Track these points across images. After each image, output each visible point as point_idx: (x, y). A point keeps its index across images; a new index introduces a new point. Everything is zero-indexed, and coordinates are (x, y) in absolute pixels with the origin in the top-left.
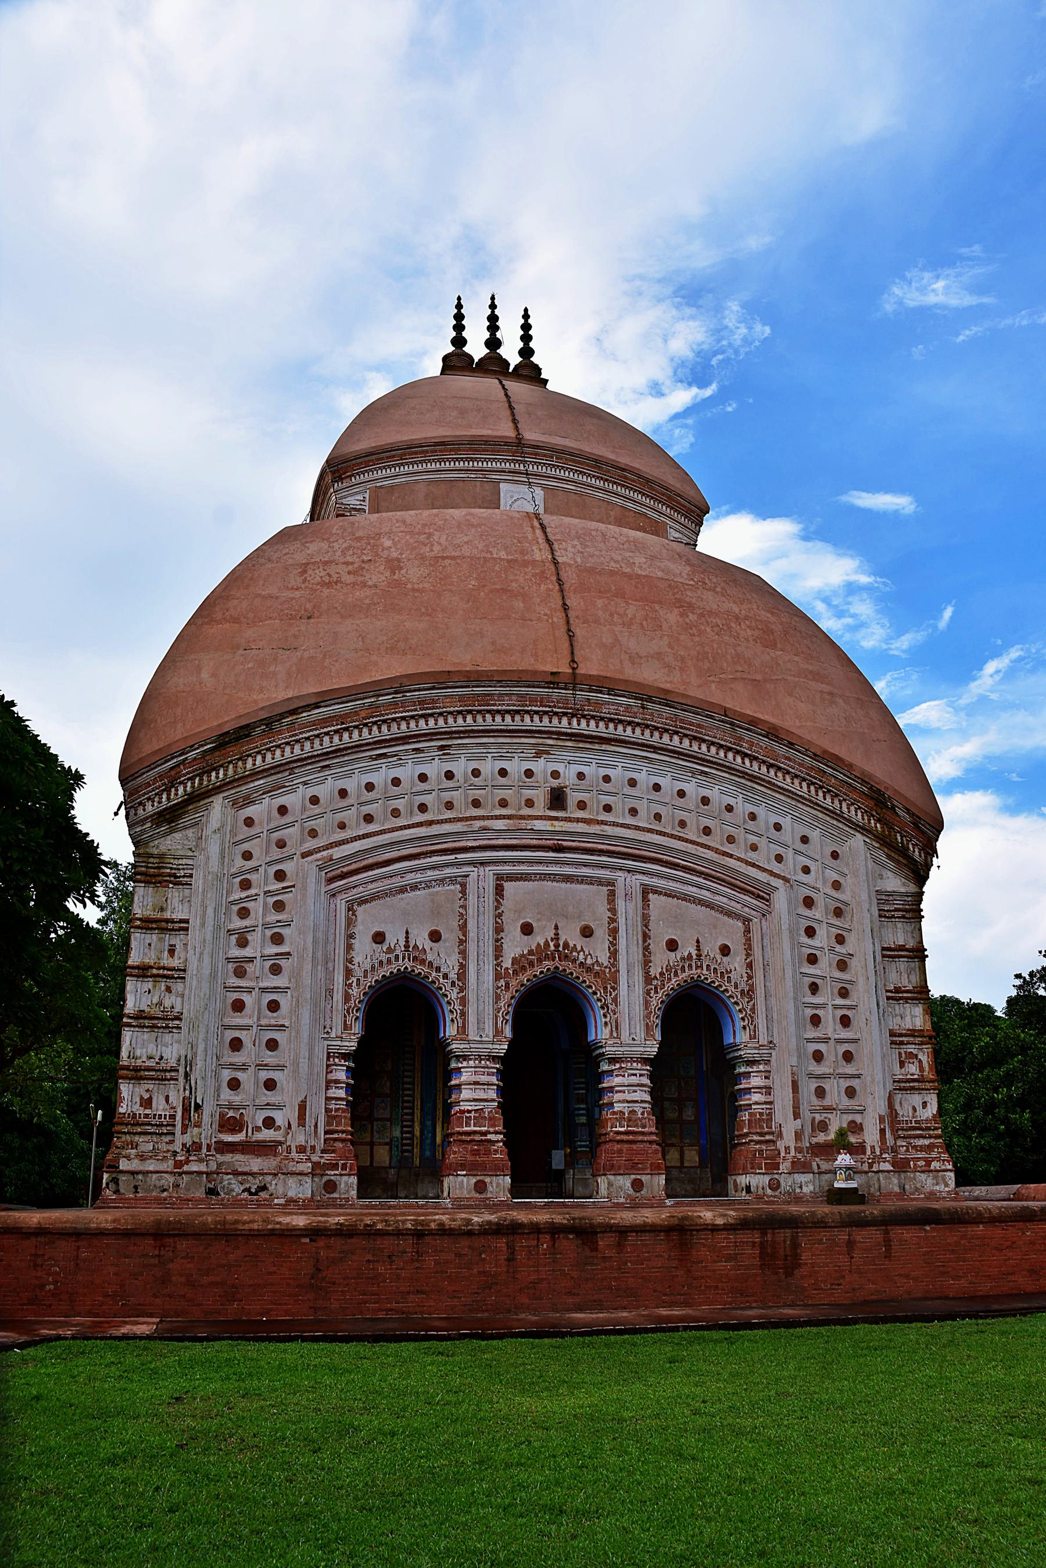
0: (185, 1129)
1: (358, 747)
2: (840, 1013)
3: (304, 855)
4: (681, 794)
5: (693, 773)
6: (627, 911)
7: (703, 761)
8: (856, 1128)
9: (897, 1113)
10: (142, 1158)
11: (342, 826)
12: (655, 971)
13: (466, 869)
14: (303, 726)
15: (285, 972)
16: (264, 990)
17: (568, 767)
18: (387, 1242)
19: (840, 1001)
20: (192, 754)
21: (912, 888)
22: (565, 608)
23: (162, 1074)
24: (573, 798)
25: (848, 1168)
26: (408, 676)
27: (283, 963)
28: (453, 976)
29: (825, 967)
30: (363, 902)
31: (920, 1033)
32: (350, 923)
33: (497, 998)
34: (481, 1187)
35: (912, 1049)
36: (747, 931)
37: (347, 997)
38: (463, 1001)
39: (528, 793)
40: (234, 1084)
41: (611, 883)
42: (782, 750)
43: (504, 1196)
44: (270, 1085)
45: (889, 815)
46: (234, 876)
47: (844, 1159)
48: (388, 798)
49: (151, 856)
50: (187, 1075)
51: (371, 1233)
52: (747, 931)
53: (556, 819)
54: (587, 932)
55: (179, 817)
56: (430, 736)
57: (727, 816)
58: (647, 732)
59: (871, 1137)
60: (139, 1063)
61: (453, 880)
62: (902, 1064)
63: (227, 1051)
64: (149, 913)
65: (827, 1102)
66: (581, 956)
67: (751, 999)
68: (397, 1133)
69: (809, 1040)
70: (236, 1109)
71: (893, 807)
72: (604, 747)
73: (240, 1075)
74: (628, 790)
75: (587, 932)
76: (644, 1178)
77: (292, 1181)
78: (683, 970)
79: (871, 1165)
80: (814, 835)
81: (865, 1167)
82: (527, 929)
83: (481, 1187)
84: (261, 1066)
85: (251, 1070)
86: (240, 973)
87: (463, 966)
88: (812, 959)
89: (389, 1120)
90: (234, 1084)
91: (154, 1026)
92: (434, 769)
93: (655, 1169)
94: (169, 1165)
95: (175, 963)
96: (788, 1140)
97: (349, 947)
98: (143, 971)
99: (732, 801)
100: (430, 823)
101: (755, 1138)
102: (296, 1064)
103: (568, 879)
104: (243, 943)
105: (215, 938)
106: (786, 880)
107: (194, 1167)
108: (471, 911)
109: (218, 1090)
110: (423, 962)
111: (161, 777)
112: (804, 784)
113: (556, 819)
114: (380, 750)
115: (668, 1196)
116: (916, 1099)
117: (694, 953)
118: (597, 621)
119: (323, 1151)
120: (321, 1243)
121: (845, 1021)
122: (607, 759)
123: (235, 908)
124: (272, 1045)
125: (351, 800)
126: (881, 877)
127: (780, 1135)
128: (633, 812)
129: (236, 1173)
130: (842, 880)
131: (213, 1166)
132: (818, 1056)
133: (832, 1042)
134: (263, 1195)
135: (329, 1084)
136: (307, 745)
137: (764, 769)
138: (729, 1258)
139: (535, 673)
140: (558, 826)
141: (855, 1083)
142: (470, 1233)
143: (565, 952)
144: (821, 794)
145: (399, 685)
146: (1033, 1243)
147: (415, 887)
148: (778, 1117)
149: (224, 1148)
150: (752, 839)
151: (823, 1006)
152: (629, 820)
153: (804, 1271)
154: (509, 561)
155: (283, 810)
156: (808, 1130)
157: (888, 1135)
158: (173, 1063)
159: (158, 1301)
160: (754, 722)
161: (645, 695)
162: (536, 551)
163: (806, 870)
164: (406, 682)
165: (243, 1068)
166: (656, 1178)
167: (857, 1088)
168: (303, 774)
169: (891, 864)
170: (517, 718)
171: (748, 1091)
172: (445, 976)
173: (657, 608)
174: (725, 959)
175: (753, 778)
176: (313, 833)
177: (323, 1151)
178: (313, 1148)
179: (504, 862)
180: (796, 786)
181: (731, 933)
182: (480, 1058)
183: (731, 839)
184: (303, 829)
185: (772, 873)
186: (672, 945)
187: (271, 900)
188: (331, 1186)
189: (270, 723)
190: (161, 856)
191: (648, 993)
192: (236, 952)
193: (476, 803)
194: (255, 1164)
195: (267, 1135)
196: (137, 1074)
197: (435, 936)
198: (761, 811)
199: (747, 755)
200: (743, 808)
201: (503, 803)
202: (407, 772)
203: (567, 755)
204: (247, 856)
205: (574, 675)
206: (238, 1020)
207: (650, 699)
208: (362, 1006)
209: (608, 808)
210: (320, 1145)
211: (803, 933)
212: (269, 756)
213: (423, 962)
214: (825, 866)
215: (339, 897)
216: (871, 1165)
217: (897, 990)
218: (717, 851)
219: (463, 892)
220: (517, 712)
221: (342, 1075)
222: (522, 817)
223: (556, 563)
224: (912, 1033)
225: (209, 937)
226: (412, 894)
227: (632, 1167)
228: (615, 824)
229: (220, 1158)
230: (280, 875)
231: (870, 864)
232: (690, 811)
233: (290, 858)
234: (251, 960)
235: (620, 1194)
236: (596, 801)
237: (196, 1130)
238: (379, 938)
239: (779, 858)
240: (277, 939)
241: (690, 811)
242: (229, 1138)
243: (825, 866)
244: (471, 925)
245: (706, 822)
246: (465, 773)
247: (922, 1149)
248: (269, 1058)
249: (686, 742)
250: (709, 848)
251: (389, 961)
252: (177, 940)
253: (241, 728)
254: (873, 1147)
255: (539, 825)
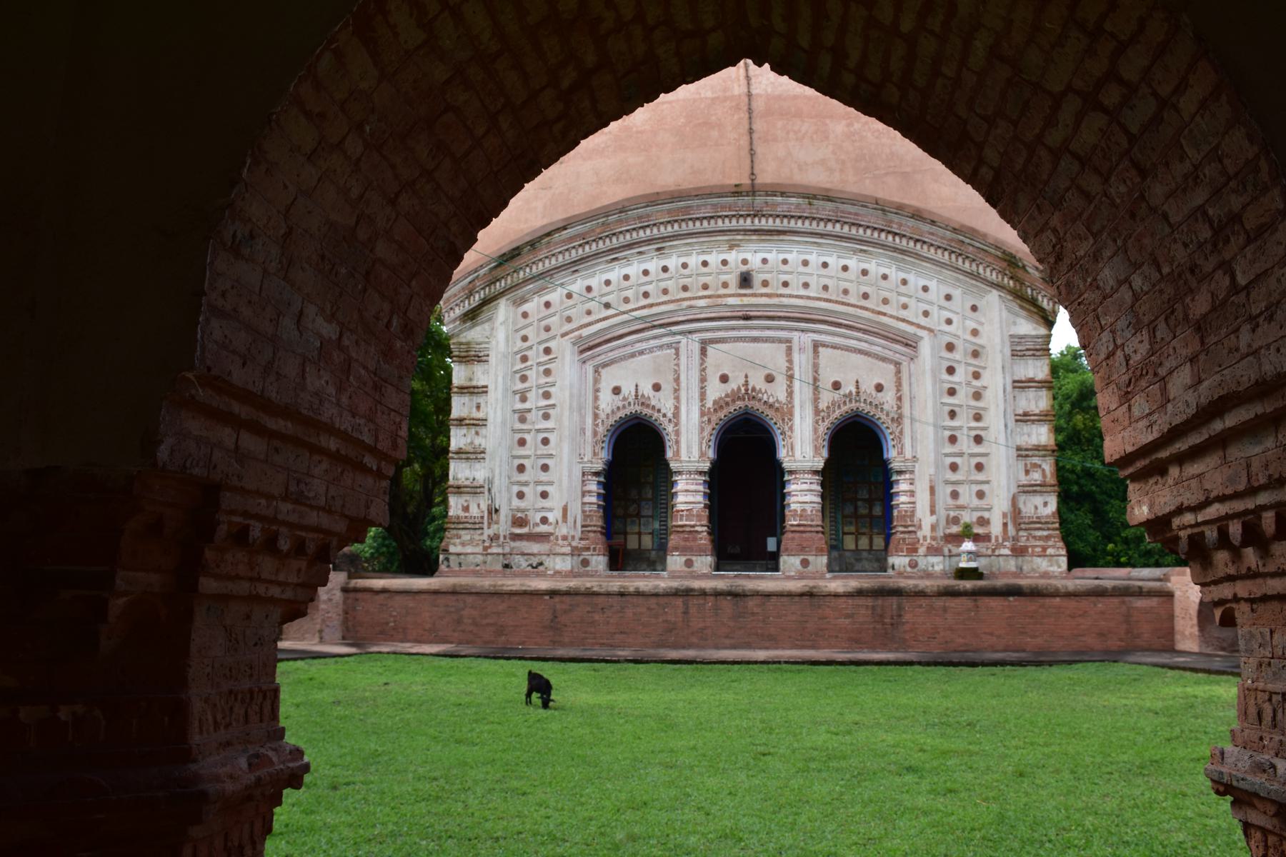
0: (489, 524)
1: (597, 255)
2: (974, 433)
3: (563, 335)
4: (845, 268)
5: (855, 251)
6: (802, 362)
7: (861, 242)
8: (983, 522)
9: (1020, 512)
10: (463, 544)
11: (589, 313)
12: (823, 405)
13: (678, 337)
14: (557, 243)
15: (552, 418)
16: (538, 431)
17: (753, 255)
18: (601, 599)
19: (974, 424)
20: (482, 272)
21: (1042, 331)
22: (751, 131)
23: (475, 490)
24: (757, 279)
25: (970, 553)
26: (628, 200)
27: (551, 411)
28: (670, 415)
29: (962, 398)
30: (605, 365)
31: (1045, 448)
32: (596, 381)
33: (702, 430)
34: (689, 563)
35: (1036, 460)
36: (898, 372)
37: (595, 433)
38: (677, 433)
39: (724, 278)
40: (521, 495)
41: (789, 341)
42: (926, 227)
43: (706, 570)
44: (544, 495)
45: (1020, 274)
46: (516, 353)
47: (968, 546)
48: (621, 290)
49: (461, 344)
50: (489, 490)
51: (590, 594)
52: (898, 372)
53: (745, 295)
54: (770, 379)
55: (477, 315)
56: (649, 241)
57: (883, 283)
58: (814, 223)
59: (996, 529)
60: (460, 483)
61: (669, 346)
62: (1027, 472)
63: (515, 473)
64: (464, 383)
65: (961, 502)
66: (765, 398)
67: (899, 424)
68: (657, 525)
69: (946, 455)
70: (523, 511)
71: (1024, 267)
72: (781, 237)
73: (524, 489)
74: (802, 269)
75: (770, 379)
76: (811, 558)
77: (558, 559)
78: (845, 403)
79: (993, 550)
80: (957, 293)
81: (989, 552)
82: (724, 379)
83: (689, 563)
84: (538, 483)
85: (532, 485)
86: (523, 420)
87: (677, 408)
88: (952, 392)
89: (652, 517)
90: (521, 495)
91: (467, 459)
92: (653, 265)
93: (819, 551)
94: (479, 549)
95: (480, 415)
96: (926, 531)
97: (596, 398)
98: (461, 422)
99: (886, 271)
100: (651, 306)
101: (901, 529)
102: (560, 481)
103: (755, 340)
104: (524, 399)
105: (505, 397)
106: (930, 330)
107: (494, 550)
108: (683, 368)
109: (510, 501)
110: (648, 406)
111: (463, 289)
112: (946, 253)
113: (745, 295)
114: (613, 255)
115: (830, 570)
116: (1038, 500)
117: (854, 390)
118: (775, 140)
119: (581, 539)
120: (557, 599)
121: (978, 440)
122: (786, 247)
123: (518, 376)
124: (545, 468)
125: (594, 294)
126: (1015, 323)
127: (920, 527)
128: (806, 285)
129: (523, 554)
130: (979, 328)
131: (507, 550)
132: (954, 467)
133: (966, 456)
134: (541, 568)
135: (584, 494)
136: (560, 257)
137: (912, 244)
138: (848, 616)
139: (722, 186)
140: (746, 300)
141: (984, 487)
142: (656, 595)
143: (751, 393)
144: (960, 260)
145: (622, 208)
146: (1103, 613)
147: (641, 353)
148: (919, 514)
149: (515, 537)
150: (904, 300)
151: (960, 428)
152: (802, 292)
153: (907, 627)
154: (713, 99)
155: (548, 305)
156: (943, 523)
157: (1010, 527)
158: (481, 482)
159: (456, 634)
160: (900, 209)
161: (811, 196)
162: (736, 87)
163: (949, 322)
164: (626, 204)
165: (526, 484)
166: (819, 558)
167: (987, 492)
168: (559, 278)
169: (1024, 313)
170: (712, 221)
171: (897, 494)
172: (664, 416)
173: (828, 121)
174: (879, 395)
175: (903, 252)
176: (569, 319)
177: (581, 539)
178: (573, 537)
179: (707, 330)
180: (939, 255)
181: (885, 374)
182: (690, 473)
183: (885, 301)
184: (561, 317)
185: (919, 326)
186: (837, 386)
187: (542, 369)
188: (585, 563)
189: (533, 244)
190: (468, 343)
191: (817, 422)
192: (519, 406)
193: (685, 288)
194: (535, 547)
195: (543, 529)
196: (459, 490)
197: (657, 387)
198: (911, 278)
199: (896, 234)
200: (895, 275)
201: (705, 287)
202: (634, 269)
203: (753, 246)
204: (525, 339)
205: (753, 185)
206: (522, 451)
207: (815, 197)
208: (607, 439)
209: (785, 284)
210: (578, 534)
211: (944, 371)
212: (534, 267)
213: (648, 406)
214: (965, 318)
215: (589, 363)
216: (993, 550)
217: (1025, 414)
218: (873, 311)
219: (677, 354)
220: (712, 217)
221: (593, 486)
222: (719, 296)
223: (749, 95)
224: (1037, 448)
225: (500, 396)
226: (640, 358)
227: (802, 549)
228: (791, 296)
229: (513, 544)
230: (547, 351)
231: (1005, 313)
232: (851, 281)
233: (554, 338)
234: (529, 410)
235: (799, 569)
236: (776, 280)
237: (495, 526)
238: (617, 391)
239: (926, 314)
240: (547, 395)
241: (851, 281)
242: (518, 531)
243: (965, 318)
244: (683, 378)
245: (864, 289)
246: (676, 267)
247: (1040, 538)
248: (544, 477)
249: (846, 228)
250: (866, 309)
251: (624, 407)
252: (481, 399)
253: (514, 249)
254: (997, 537)
255: (731, 301)
